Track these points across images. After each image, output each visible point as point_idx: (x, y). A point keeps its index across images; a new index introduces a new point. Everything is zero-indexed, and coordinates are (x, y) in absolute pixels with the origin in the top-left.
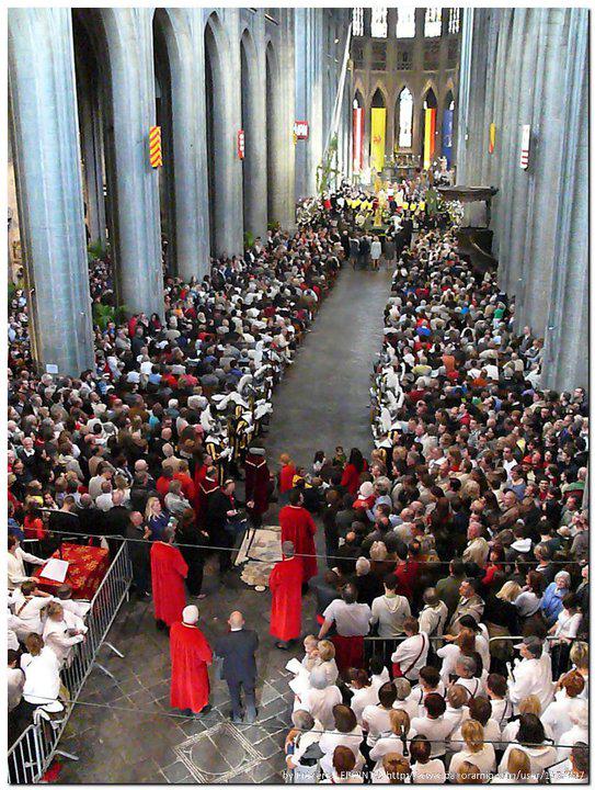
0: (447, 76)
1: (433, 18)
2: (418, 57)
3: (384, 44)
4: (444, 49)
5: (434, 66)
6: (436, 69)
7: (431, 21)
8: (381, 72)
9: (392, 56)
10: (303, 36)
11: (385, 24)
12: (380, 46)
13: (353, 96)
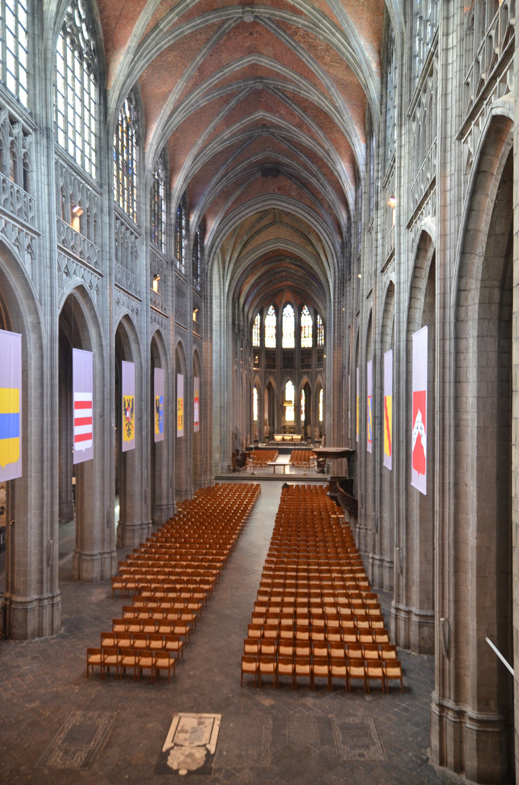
0: (318, 373)
2: (297, 362)
3: (274, 352)
5: (309, 366)
6: (309, 368)
7: (305, 337)
8: (273, 370)
9: (279, 361)
12: (269, 352)
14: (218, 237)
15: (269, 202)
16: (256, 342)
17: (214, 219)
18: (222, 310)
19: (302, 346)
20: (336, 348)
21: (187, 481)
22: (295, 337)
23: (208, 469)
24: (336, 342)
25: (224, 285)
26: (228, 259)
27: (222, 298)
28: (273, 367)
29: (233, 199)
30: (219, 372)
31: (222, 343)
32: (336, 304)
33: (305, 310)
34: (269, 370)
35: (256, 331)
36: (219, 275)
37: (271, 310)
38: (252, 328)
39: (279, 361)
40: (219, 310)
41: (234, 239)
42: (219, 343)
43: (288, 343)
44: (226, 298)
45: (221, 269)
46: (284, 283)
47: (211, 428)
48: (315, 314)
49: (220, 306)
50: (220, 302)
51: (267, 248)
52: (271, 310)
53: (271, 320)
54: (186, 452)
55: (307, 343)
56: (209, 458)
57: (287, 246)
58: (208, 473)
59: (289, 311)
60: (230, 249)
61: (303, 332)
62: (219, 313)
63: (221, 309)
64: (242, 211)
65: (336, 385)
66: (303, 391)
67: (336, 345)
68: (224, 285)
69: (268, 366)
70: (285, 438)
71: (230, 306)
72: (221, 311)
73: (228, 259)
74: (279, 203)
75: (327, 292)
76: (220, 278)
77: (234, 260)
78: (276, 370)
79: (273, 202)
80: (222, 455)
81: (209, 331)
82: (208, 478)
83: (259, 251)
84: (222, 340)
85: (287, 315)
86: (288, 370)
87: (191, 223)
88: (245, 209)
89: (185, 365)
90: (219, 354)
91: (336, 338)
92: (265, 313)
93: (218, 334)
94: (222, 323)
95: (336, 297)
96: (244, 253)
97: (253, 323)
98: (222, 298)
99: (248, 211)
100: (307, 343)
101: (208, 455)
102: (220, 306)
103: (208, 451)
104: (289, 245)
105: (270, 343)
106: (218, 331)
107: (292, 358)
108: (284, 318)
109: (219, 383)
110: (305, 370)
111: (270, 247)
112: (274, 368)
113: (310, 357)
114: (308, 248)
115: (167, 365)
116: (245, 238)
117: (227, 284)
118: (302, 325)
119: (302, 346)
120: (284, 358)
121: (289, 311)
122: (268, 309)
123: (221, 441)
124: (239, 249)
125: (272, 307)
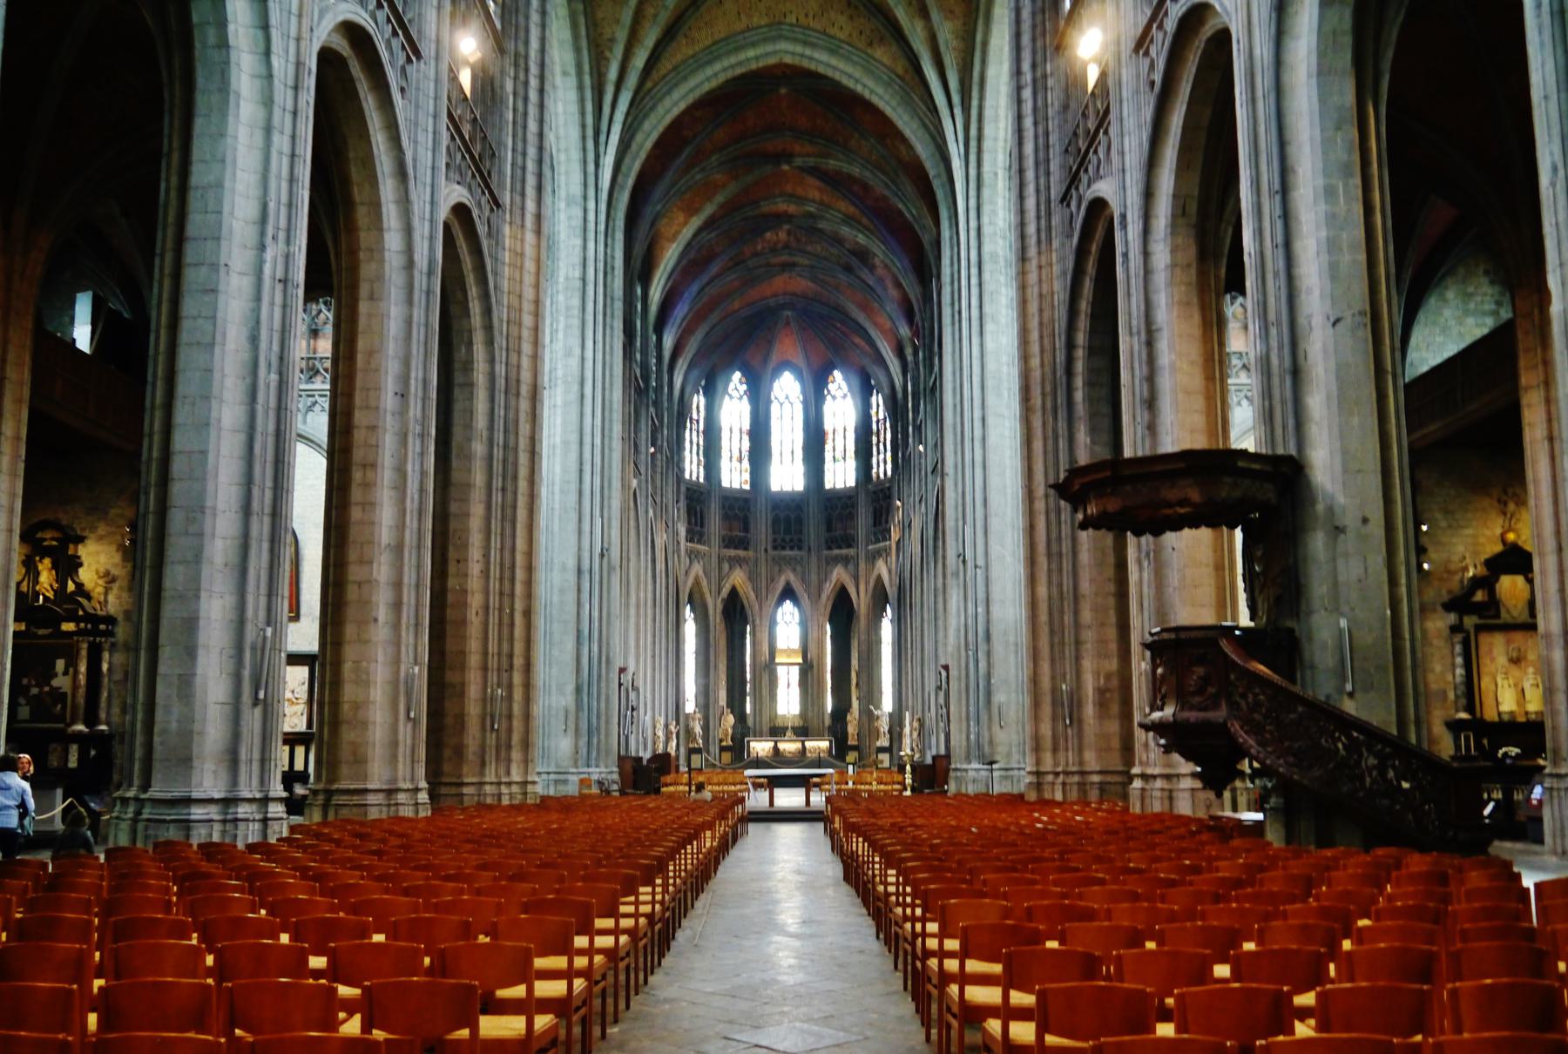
0: (873, 558)
1: (839, 455)
3: (746, 501)
5: (849, 541)
6: (849, 546)
8: (741, 553)
9: (762, 531)
10: (574, 362)
11: (746, 464)
13: (684, 597)
16: (693, 468)
18: (591, 245)
19: (828, 486)
20: (1032, 251)
21: (394, 744)
23: (516, 738)
24: (1031, 229)
25: (597, 165)
26: (613, 74)
27: (591, 205)
28: (743, 544)
30: (575, 447)
31: (589, 354)
32: (1027, 94)
33: (839, 384)
34: (732, 552)
35: (693, 439)
36: (583, 126)
38: (681, 427)
39: (762, 531)
40: (578, 242)
42: (577, 351)
43: (787, 476)
44: (603, 207)
46: (780, 283)
47: (530, 569)
48: (865, 389)
49: (585, 230)
51: (742, 56)
53: (734, 410)
54: (397, 605)
55: (841, 474)
56: (518, 694)
57: (808, 52)
58: (516, 755)
59: (787, 388)
60: (622, 35)
61: (828, 447)
62: (578, 251)
63: (585, 240)
66: (828, 627)
67: (1032, 241)
68: (597, 165)
69: (729, 542)
70: (782, 746)
71: (618, 325)
72: (585, 248)
73: (613, 74)
75: (940, 195)
76: (584, 138)
77: (632, 80)
78: (751, 553)
80: (583, 741)
81: (530, 192)
82: (516, 776)
83: (717, 67)
84: (589, 344)
86: (788, 553)
89: (405, 202)
90: (576, 388)
92: (720, 386)
93: (576, 322)
96: (665, 65)
97: (682, 416)
98: (591, 205)
101: (517, 678)
102: (585, 230)
103: (518, 661)
104: (813, 46)
105: (734, 476)
106: (576, 312)
107: (799, 521)
109: (574, 487)
110: (836, 552)
111: (751, 53)
112: (746, 549)
114: (879, 53)
115: (265, 27)
117: (608, 161)
118: (828, 426)
119: (828, 486)
121: (787, 388)
122: (729, 380)
123: (578, 690)
124: (650, 38)
125: (737, 375)
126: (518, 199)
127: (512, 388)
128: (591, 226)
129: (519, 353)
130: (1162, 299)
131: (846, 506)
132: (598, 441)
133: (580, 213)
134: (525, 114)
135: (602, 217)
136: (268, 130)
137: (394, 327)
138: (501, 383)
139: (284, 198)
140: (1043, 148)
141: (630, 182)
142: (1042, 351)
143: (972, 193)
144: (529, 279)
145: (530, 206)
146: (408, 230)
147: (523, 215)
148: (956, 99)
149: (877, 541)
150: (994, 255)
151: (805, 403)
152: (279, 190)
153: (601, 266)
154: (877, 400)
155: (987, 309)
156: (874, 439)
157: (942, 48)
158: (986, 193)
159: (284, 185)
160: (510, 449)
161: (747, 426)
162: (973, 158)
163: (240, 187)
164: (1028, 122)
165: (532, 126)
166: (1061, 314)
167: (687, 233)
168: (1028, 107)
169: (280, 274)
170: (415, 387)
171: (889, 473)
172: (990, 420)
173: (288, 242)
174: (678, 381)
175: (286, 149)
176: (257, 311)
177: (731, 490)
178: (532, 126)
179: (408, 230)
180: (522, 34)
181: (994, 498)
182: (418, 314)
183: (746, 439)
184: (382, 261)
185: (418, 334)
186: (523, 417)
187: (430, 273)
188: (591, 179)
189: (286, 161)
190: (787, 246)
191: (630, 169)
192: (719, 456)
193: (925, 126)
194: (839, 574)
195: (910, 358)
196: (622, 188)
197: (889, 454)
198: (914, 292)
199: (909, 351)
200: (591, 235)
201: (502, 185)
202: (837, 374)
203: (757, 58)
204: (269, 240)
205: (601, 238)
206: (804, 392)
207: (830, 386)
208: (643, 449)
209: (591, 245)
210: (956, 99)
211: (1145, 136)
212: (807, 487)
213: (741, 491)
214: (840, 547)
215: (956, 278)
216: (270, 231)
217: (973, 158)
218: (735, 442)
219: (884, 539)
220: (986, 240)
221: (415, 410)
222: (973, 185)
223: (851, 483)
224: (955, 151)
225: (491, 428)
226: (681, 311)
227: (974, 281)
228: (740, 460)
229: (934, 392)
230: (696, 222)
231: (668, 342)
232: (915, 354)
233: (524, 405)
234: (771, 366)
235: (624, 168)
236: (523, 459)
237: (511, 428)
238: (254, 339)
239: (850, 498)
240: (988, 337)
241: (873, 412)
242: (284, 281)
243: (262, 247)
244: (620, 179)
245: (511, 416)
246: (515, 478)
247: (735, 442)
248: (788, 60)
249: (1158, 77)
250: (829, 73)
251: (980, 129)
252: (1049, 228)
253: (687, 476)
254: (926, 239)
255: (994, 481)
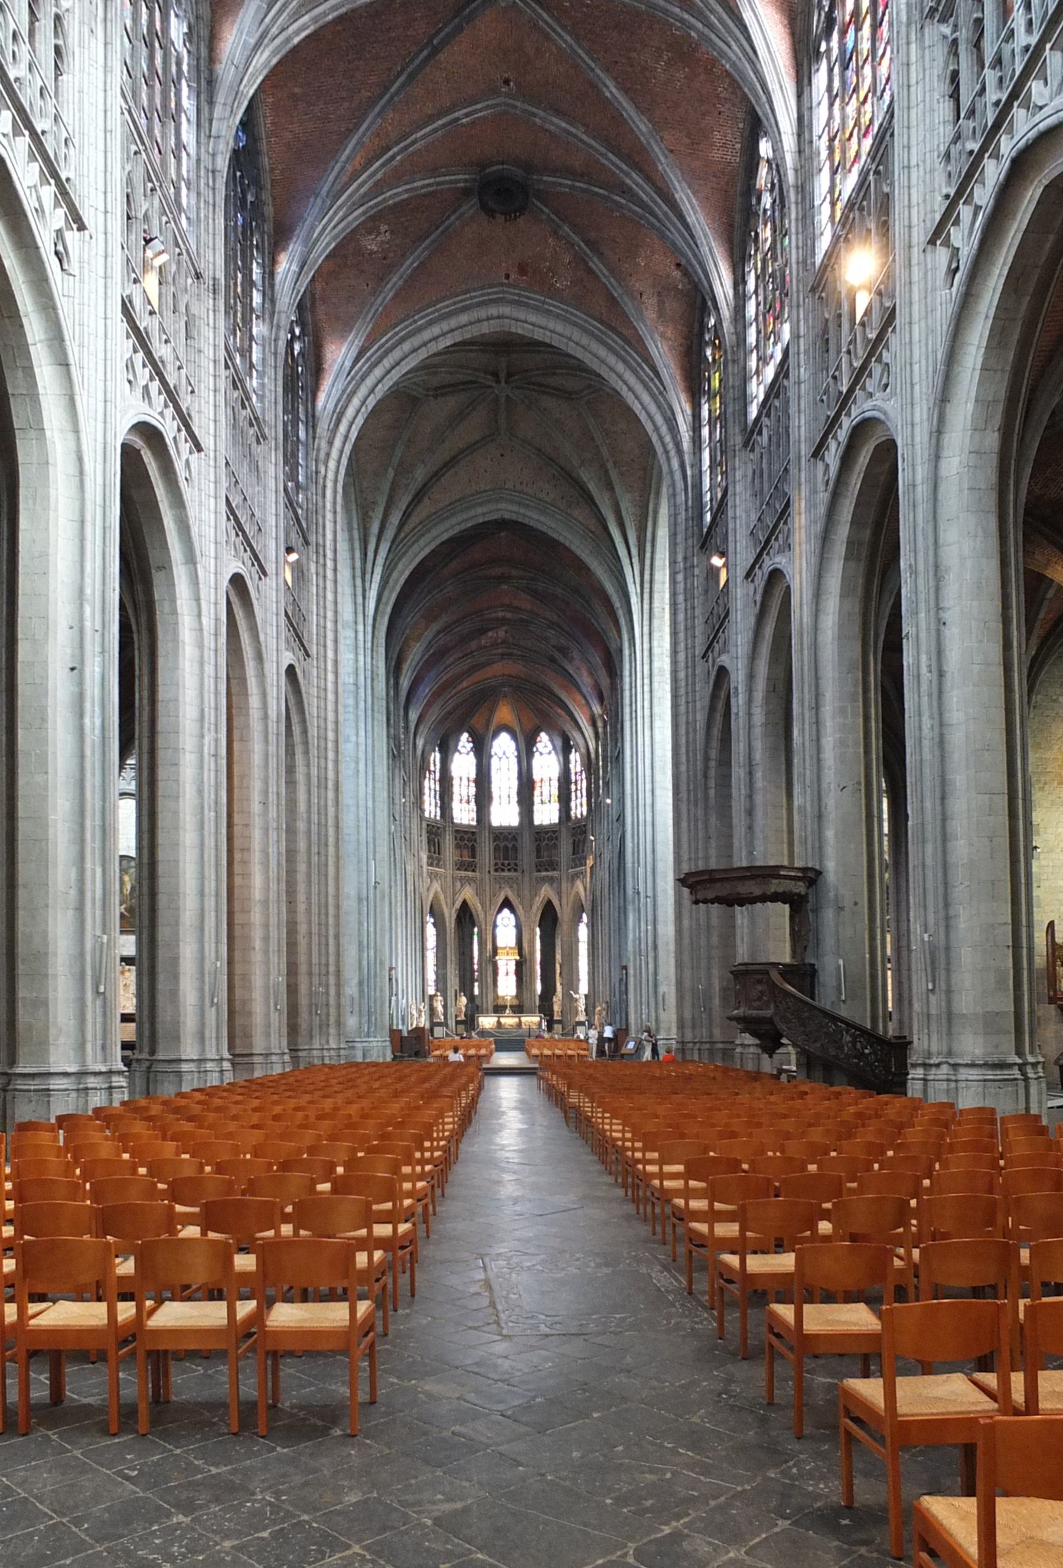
0: (573, 878)
1: (546, 798)
2: (526, 856)
3: (473, 833)
4: (565, 847)
5: (552, 865)
11: (473, 805)
14: (354, 393)
15: (493, 311)
16: (431, 808)
17: (344, 338)
18: (361, 658)
19: (537, 822)
22: (520, 802)
25: (364, 597)
27: (361, 628)
29: (395, 280)
32: (680, 577)
35: (431, 786)
37: (464, 741)
40: (352, 656)
41: (391, 473)
44: (369, 629)
45: (358, 554)
48: (566, 749)
49: (356, 647)
50: (356, 638)
52: (464, 741)
55: (546, 814)
57: (522, 511)
59: (504, 746)
61: (537, 793)
63: (357, 654)
64: (420, 330)
65: (683, 788)
68: (364, 597)
72: (357, 661)
74: (521, 314)
76: (354, 577)
79: (506, 310)
84: (362, 733)
85: (500, 754)
87: (278, 278)
88: (431, 323)
91: (682, 665)
92: (452, 746)
94: (362, 691)
95: (680, 558)
97: (424, 768)
99: (436, 330)
100: (546, 814)
102: (356, 647)
104: (527, 506)
105: (464, 814)
107: (515, 849)
108: (494, 762)
110: (544, 873)
113: (555, 846)
114: (576, 513)
116: (420, 474)
117: (373, 594)
118: (536, 776)
119: (537, 822)
120: (497, 849)
121: (504, 746)
122: (458, 741)
125: (465, 736)
126: (322, 649)
127: (322, 784)
128: (361, 644)
129: (326, 758)
130: (758, 745)
131: (551, 839)
132: (370, 804)
133: (353, 635)
134: (325, 588)
135: (369, 637)
136: (202, 663)
137: (257, 758)
138: (314, 781)
139: (213, 705)
140: (691, 618)
141: (389, 610)
142: (688, 761)
143: (646, 622)
144: (330, 707)
145: (330, 654)
146: (264, 695)
147: (325, 662)
148: (634, 551)
149: (576, 866)
150: (661, 670)
151: (519, 757)
152: (210, 698)
153: (369, 674)
154: (575, 757)
155: (656, 710)
156: (573, 787)
157: (624, 513)
158: (656, 623)
159: (212, 696)
160: (322, 826)
161: (473, 775)
162: (646, 596)
163: (188, 699)
164: (681, 598)
165: (330, 596)
166: (700, 736)
167: (429, 635)
168: (680, 587)
169: (212, 752)
170: (272, 797)
171: (585, 813)
172: (658, 792)
173: (216, 732)
174: (420, 743)
175: (212, 674)
176: (201, 774)
177: (461, 825)
178: (330, 596)
179: (264, 695)
180: (321, 530)
181: (659, 847)
182: (272, 749)
183: (472, 785)
184: (248, 715)
185: (272, 763)
186: (330, 803)
187: (278, 722)
188: (360, 609)
189: (212, 681)
190: (504, 642)
191: (388, 599)
192: (451, 799)
193: (611, 570)
194: (546, 891)
195: (600, 730)
196: (384, 613)
197: (584, 799)
198: (605, 682)
199: (600, 724)
200: (361, 651)
201: (310, 641)
202: (544, 737)
203: (484, 514)
204: (206, 731)
205: (369, 652)
206: (518, 749)
207: (538, 745)
208: (397, 801)
209: (361, 658)
210: (634, 551)
211: (750, 634)
212: (521, 823)
213: (469, 826)
214: (547, 870)
215: (633, 686)
216: (206, 726)
217: (646, 596)
218: (463, 789)
219: (581, 865)
220: (655, 658)
221: (273, 813)
222: (646, 616)
223: (555, 820)
224: (633, 590)
225: (309, 811)
226: (425, 691)
227: (647, 688)
228: (468, 802)
229: (617, 759)
230: (435, 627)
231: (413, 716)
232: (605, 727)
233: (331, 795)
234: (492, 728)
235: (384, 600)
236: (331, 831)
237: (323, 811)
238: (200, 792)
239: (554, 832)
240: (656, 731)
241: (572, 766)
242: (215, 756)
243: (202, 736)
244: (381, 607)
245: (322, 803)
246: (326, 845)
247: (463, 789)
248: (507, 516)
249: (758, 598)
250: (540, 527)
251: (652, 575)
252: (694, 675)
253: (427, 815)
254: (613, 646)
255: (659, 837)
